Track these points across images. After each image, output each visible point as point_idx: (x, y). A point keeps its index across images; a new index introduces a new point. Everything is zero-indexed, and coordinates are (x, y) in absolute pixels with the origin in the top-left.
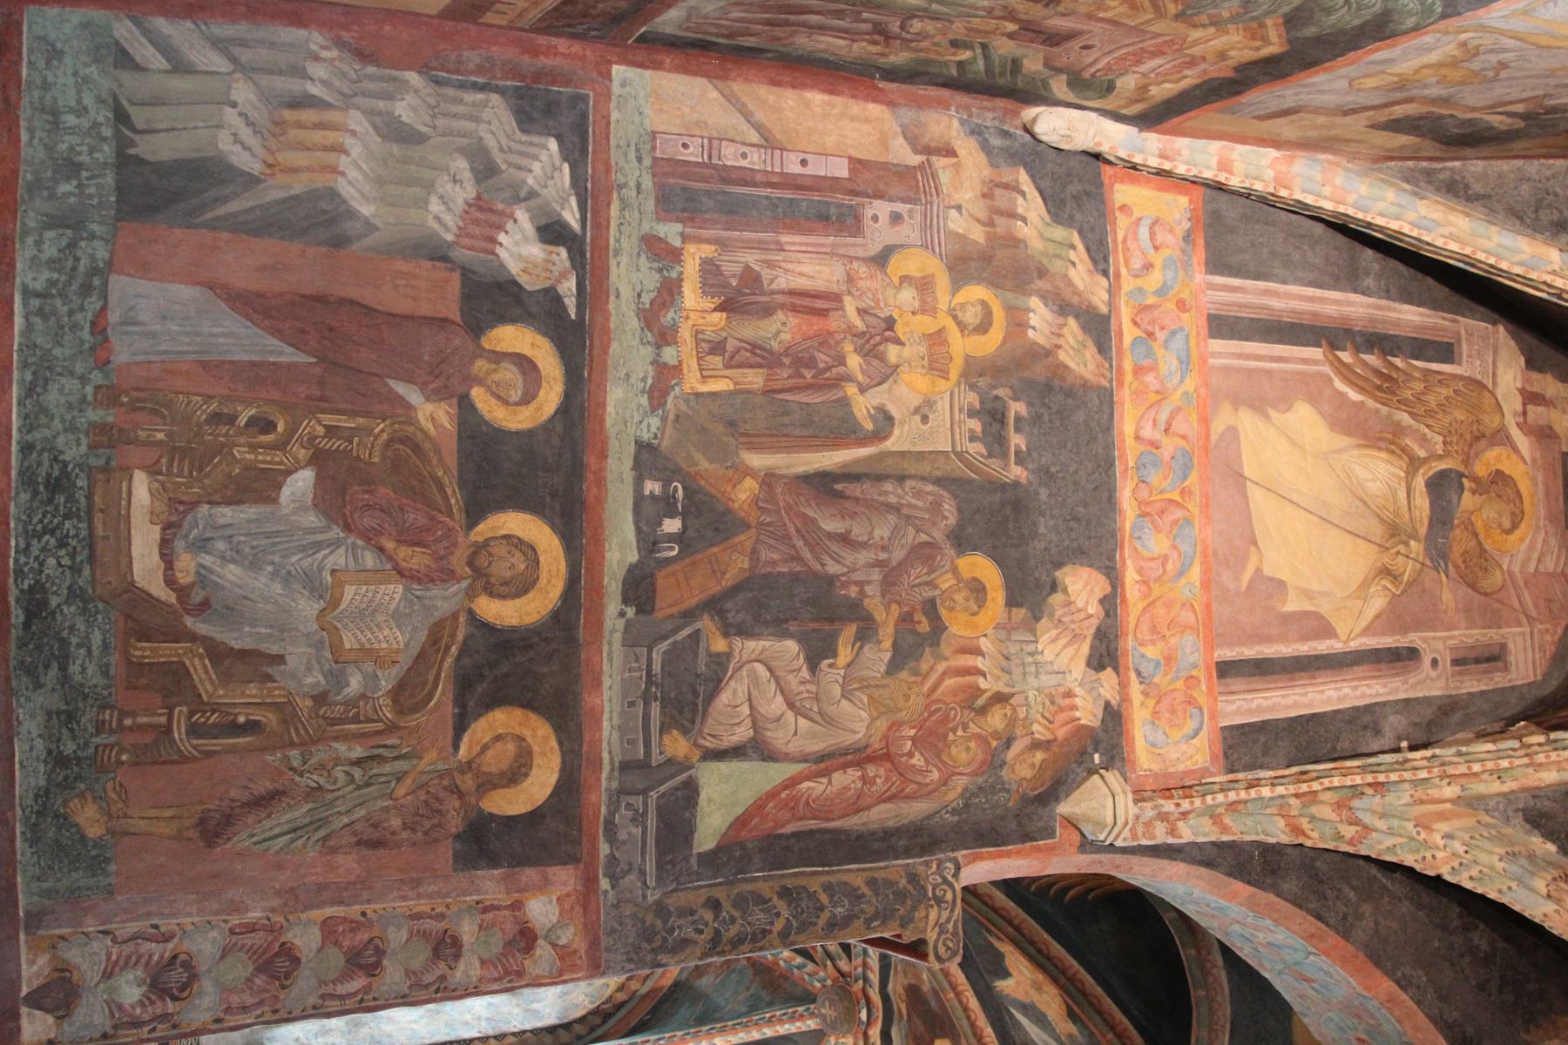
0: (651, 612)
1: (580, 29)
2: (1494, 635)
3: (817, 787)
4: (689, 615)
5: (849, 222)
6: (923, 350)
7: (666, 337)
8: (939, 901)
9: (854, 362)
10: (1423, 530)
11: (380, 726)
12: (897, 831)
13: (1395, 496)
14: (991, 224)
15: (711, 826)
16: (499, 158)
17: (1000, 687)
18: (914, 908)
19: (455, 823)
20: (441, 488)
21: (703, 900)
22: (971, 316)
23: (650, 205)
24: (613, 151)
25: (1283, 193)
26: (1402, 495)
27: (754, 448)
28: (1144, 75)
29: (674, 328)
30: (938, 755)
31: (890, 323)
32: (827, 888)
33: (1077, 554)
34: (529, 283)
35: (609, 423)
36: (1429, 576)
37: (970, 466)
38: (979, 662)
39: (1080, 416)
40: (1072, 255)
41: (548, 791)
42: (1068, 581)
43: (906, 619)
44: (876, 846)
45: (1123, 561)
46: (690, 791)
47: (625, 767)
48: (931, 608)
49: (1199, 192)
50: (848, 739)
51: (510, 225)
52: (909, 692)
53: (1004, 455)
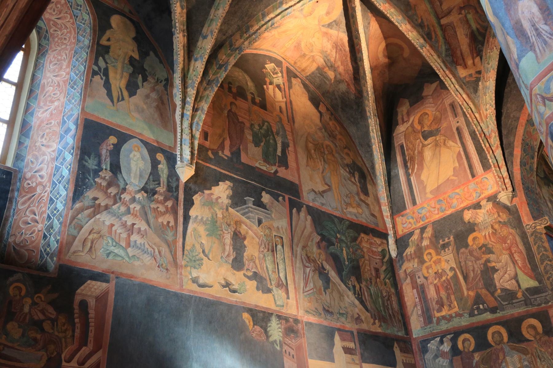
0: (497, 307)
1: (410, 346)
2: (448, 109)
3: (519, 262)
4: (496, 299)
5: (422, 286)
6: (438, 265)
7: (451, 316)
8: (535, 227)
9: (444, 278)
10: (434, 138)
11: (532, 357)
12: (523, 241)
13: (430, 148)
14: (414, 258)
15: (533, 283)
16: (434, 354)
17: (490, 228)
18: (538, 233)
19: (546, 338)
20: (488, 353)
21: (548, 281)
22: (429, 257)
23: (432, 325)
24: (426, 334)
25: (387, 204)
26: (430, 146)
27: (464, 294)
28: (377, 248)
29: (449, 315)
30: (506, 237)
31: (435, 273)
32: (539, 254)
33: (462, 219)
34: (451, 345)
35: (468, 324)
36: (442, 132)
37: (454, 248)
38: (487, 234)
39: (438, 228)
40: (413, 240)
41: (535, 320)
42: (467, 219)
43: (484, 253)
44: (527, 246)
45: (460, 208)
46: (528, 290)
47: (526, 305)
48: (480, 248)
49: (395, 217)
50: (509, 258)
51: (443, 350)
52: (497, 247)
53: (449, 242)
